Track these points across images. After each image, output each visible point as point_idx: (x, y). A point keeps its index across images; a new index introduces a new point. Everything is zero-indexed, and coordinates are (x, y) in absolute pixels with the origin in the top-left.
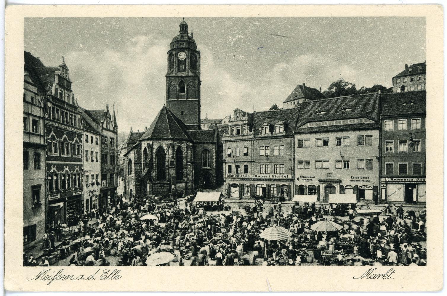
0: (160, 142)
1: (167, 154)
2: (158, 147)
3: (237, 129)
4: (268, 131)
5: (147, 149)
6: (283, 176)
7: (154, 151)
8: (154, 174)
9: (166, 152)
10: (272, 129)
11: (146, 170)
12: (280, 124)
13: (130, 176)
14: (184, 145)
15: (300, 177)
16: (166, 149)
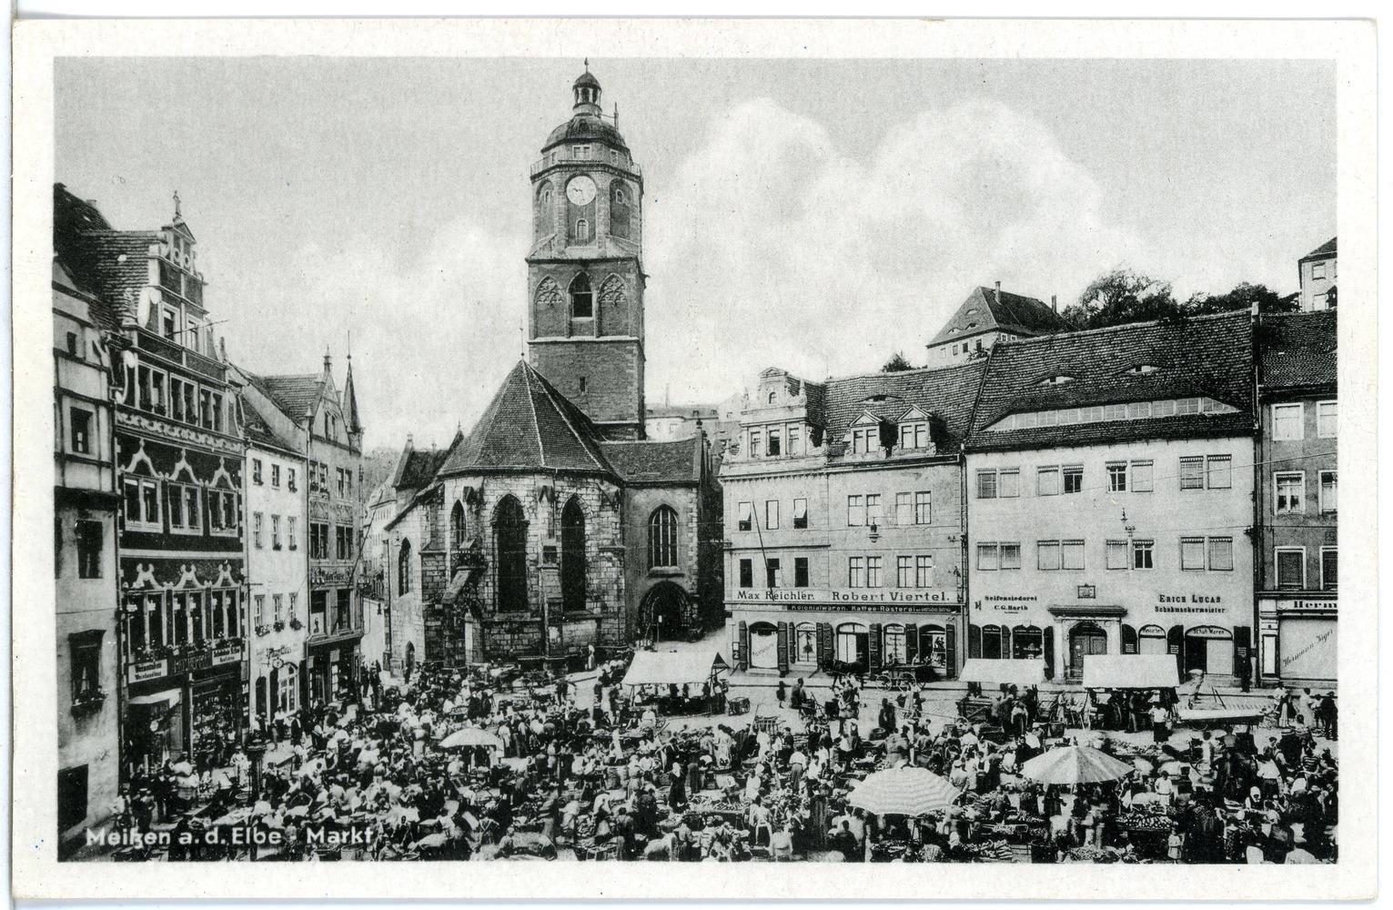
0: (508, 481)
1: (532, 522)
3: (771, 438)
4: (875, 442)
5: (465, 506)
6: (927, 595)
7: (488, 513)
8: (488, 592)
9: (527, 518)
10: (889, 434)
11: (463, 576)
12: (917, 420)
13: (407, 596)
14: (589, 491)
15: (987, 598)
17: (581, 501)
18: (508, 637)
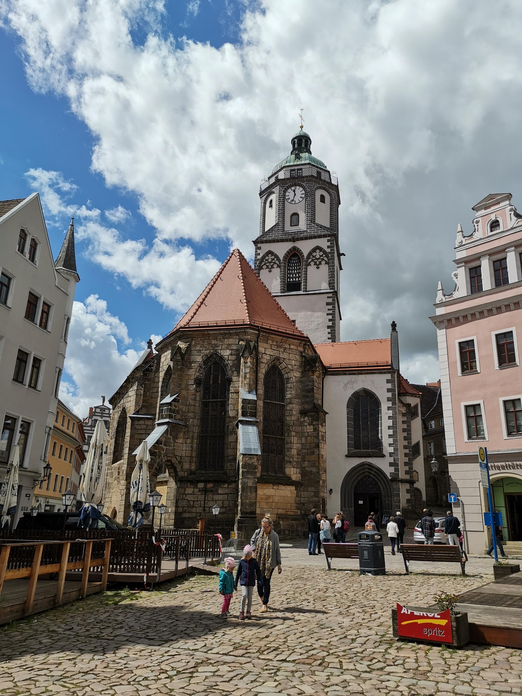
0: (214, 342)
1: (234, 379)
7: (193, 372)
17: (283, 365)
18: (202, 497)
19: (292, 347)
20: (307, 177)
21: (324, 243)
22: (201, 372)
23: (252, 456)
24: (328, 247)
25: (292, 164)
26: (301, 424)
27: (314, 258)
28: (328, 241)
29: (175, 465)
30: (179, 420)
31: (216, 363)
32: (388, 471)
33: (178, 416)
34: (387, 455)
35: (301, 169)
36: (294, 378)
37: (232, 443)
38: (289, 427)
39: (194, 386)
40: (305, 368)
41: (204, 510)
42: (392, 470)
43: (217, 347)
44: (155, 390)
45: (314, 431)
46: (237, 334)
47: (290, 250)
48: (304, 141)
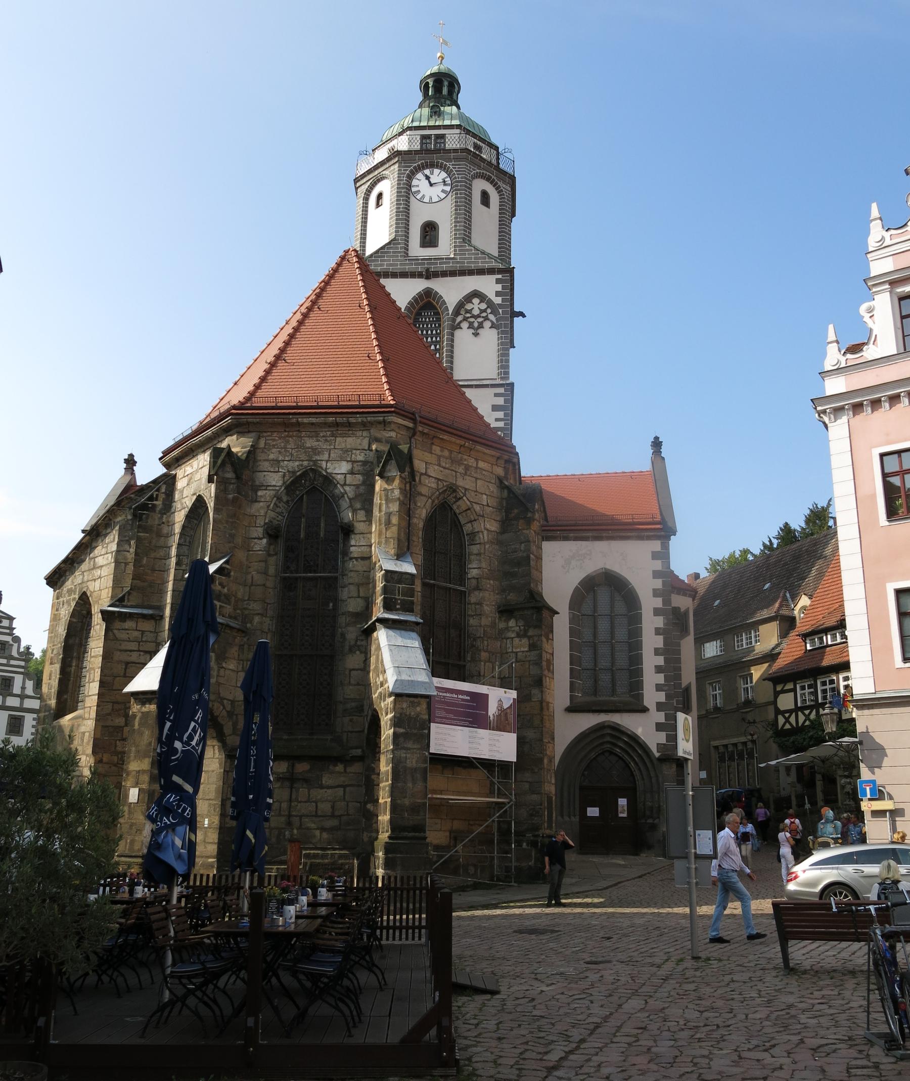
0: (310, 443)
1: (360, 527)
2: (289, 479)
7: (263, 510)
16: (350, 491)
17: (463, 504)
19: (481, 464)
20: (455, 151)
21: (489, 286)
22: (278, 510)
23: (416, 700)
24: (498, 294)
25: (424, 124)
26: (501, 635)
27: (468, 315)
28: (498, 281)
29: (220, 719)
30: (230, 617)
31: (313, 490)
32: (653, 740)
33: (228, 609)
34: (652, 707)
35: (443, 136)
36: (485, 532)
37: (353, 673)
38: (475, 640)
39: (265, 541)
40: (508, 511)
41: (289, 824)
42: (662, 737)
43: (319, 453)
44: (162, 553)
45: (530, 650)
46: (365, 426)
47: (420, 294)
48: (446, 83)
